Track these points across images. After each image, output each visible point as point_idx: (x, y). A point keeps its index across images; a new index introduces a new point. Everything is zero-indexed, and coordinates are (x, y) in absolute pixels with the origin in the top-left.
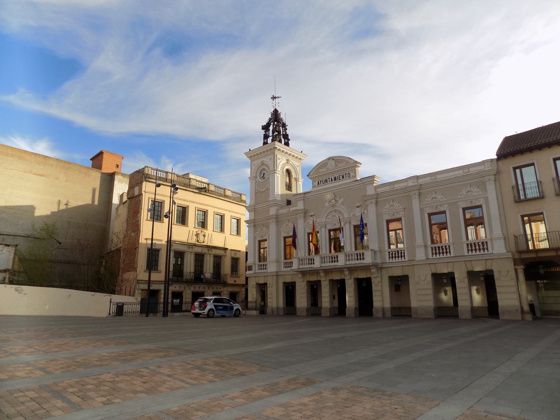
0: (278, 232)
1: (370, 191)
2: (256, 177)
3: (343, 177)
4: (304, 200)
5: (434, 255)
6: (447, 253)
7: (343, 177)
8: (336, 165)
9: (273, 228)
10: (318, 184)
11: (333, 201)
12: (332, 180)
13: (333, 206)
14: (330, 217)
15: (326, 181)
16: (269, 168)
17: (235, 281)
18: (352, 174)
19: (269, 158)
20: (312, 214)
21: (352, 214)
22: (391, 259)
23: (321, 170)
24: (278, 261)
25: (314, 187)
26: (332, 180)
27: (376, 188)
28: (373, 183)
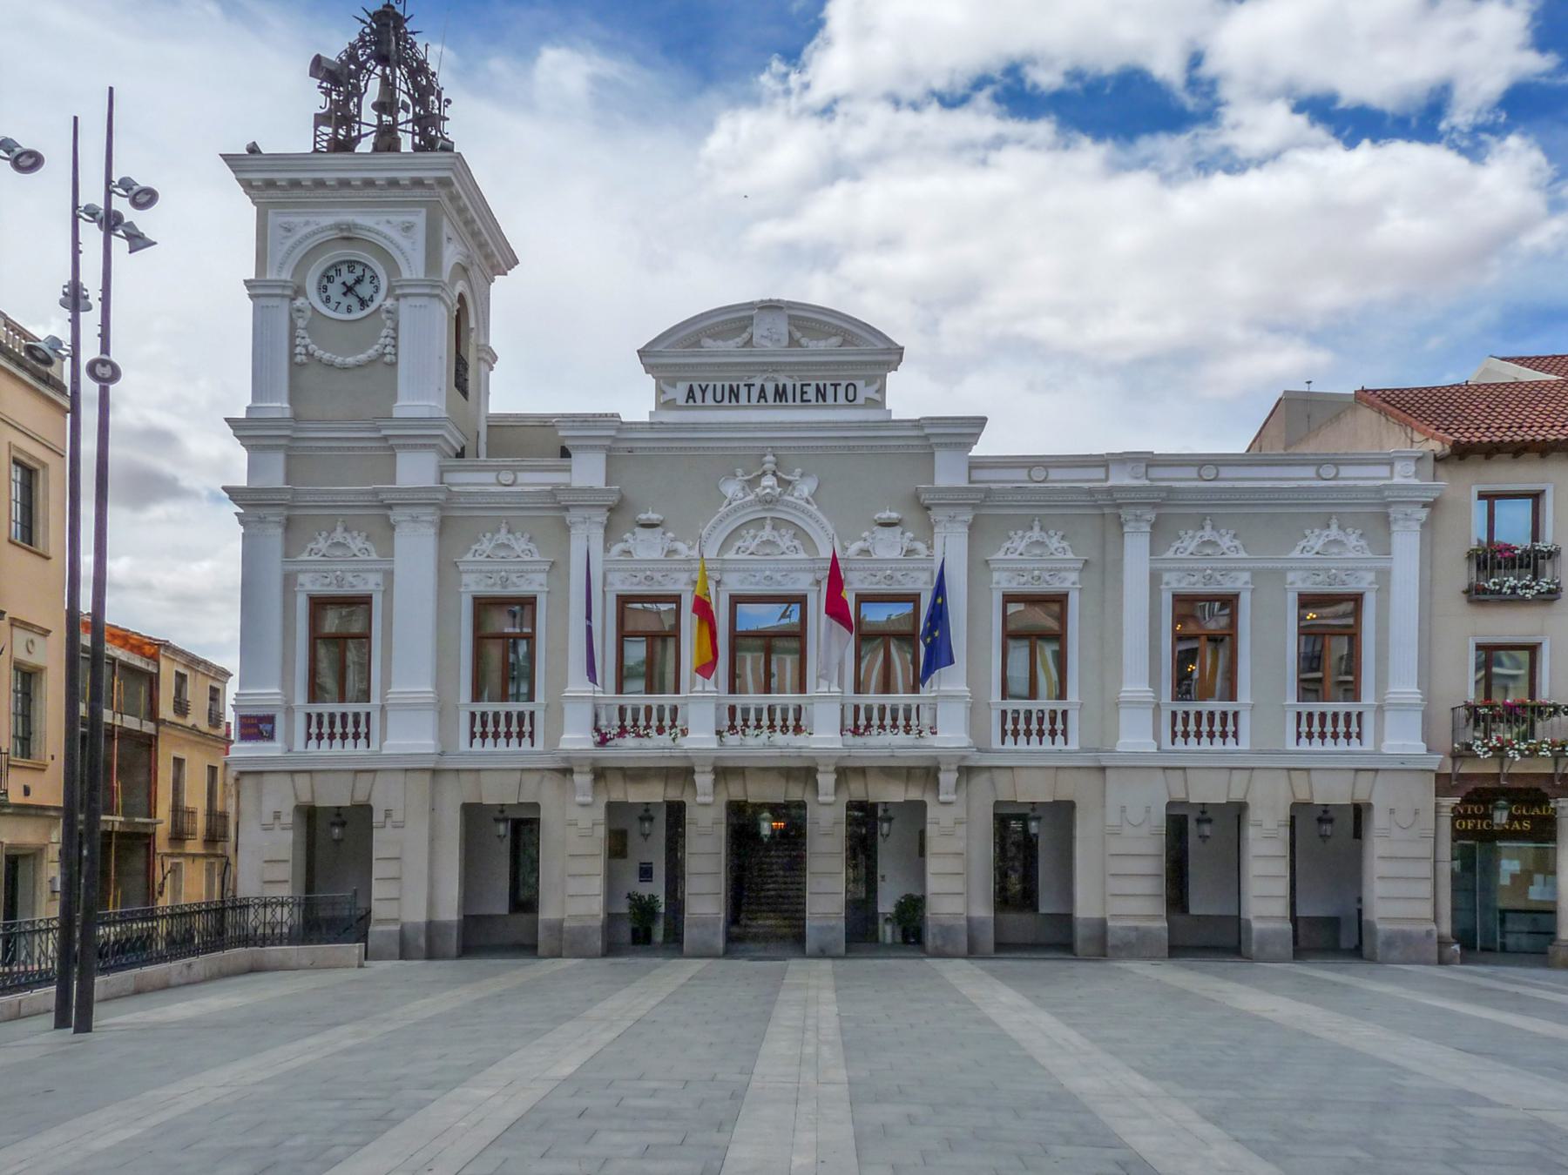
0: (447, 569)
1: (948, 474)
2: (299, 291)
3: (821, 393)
4: (609, 449)
5: (477, 741)
6: (1053, 733)
7: (821, 393)
8: (793, 342)
9: (415, 548)
10: (691, 395)
11: (769, 481)
12: (763, 395)
13: (768, 502)
14: (749, 541)
15: (734, 393)
16: (392, 267)
17: (27, 791)
18: (864, 392)
19: (399, 219)
20: (654, 516)
21: (854, 547)
22: (313, 742)
23: (709, 344)
24: (443, 709)
25: (664, 404)
26: (763, 395)
27: (977, 464)
28: (969, 446)
